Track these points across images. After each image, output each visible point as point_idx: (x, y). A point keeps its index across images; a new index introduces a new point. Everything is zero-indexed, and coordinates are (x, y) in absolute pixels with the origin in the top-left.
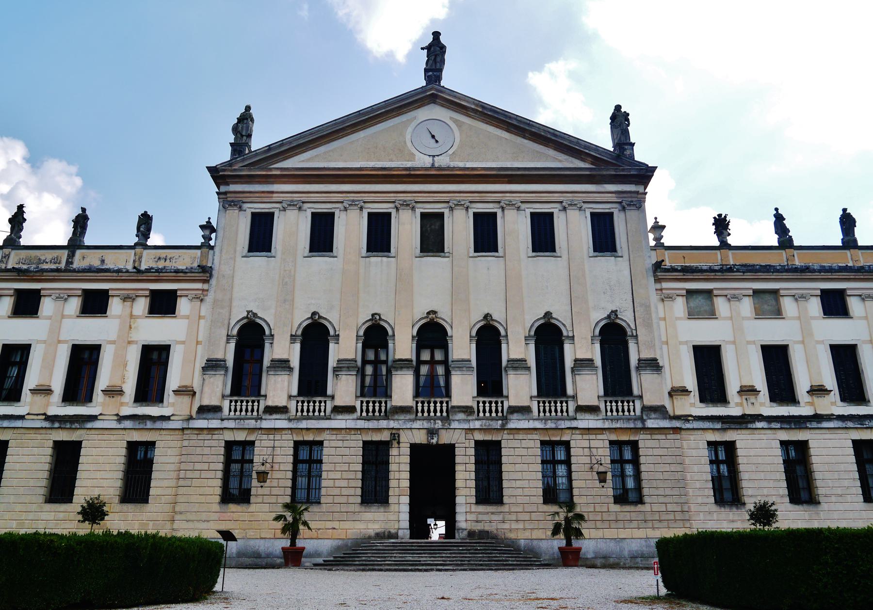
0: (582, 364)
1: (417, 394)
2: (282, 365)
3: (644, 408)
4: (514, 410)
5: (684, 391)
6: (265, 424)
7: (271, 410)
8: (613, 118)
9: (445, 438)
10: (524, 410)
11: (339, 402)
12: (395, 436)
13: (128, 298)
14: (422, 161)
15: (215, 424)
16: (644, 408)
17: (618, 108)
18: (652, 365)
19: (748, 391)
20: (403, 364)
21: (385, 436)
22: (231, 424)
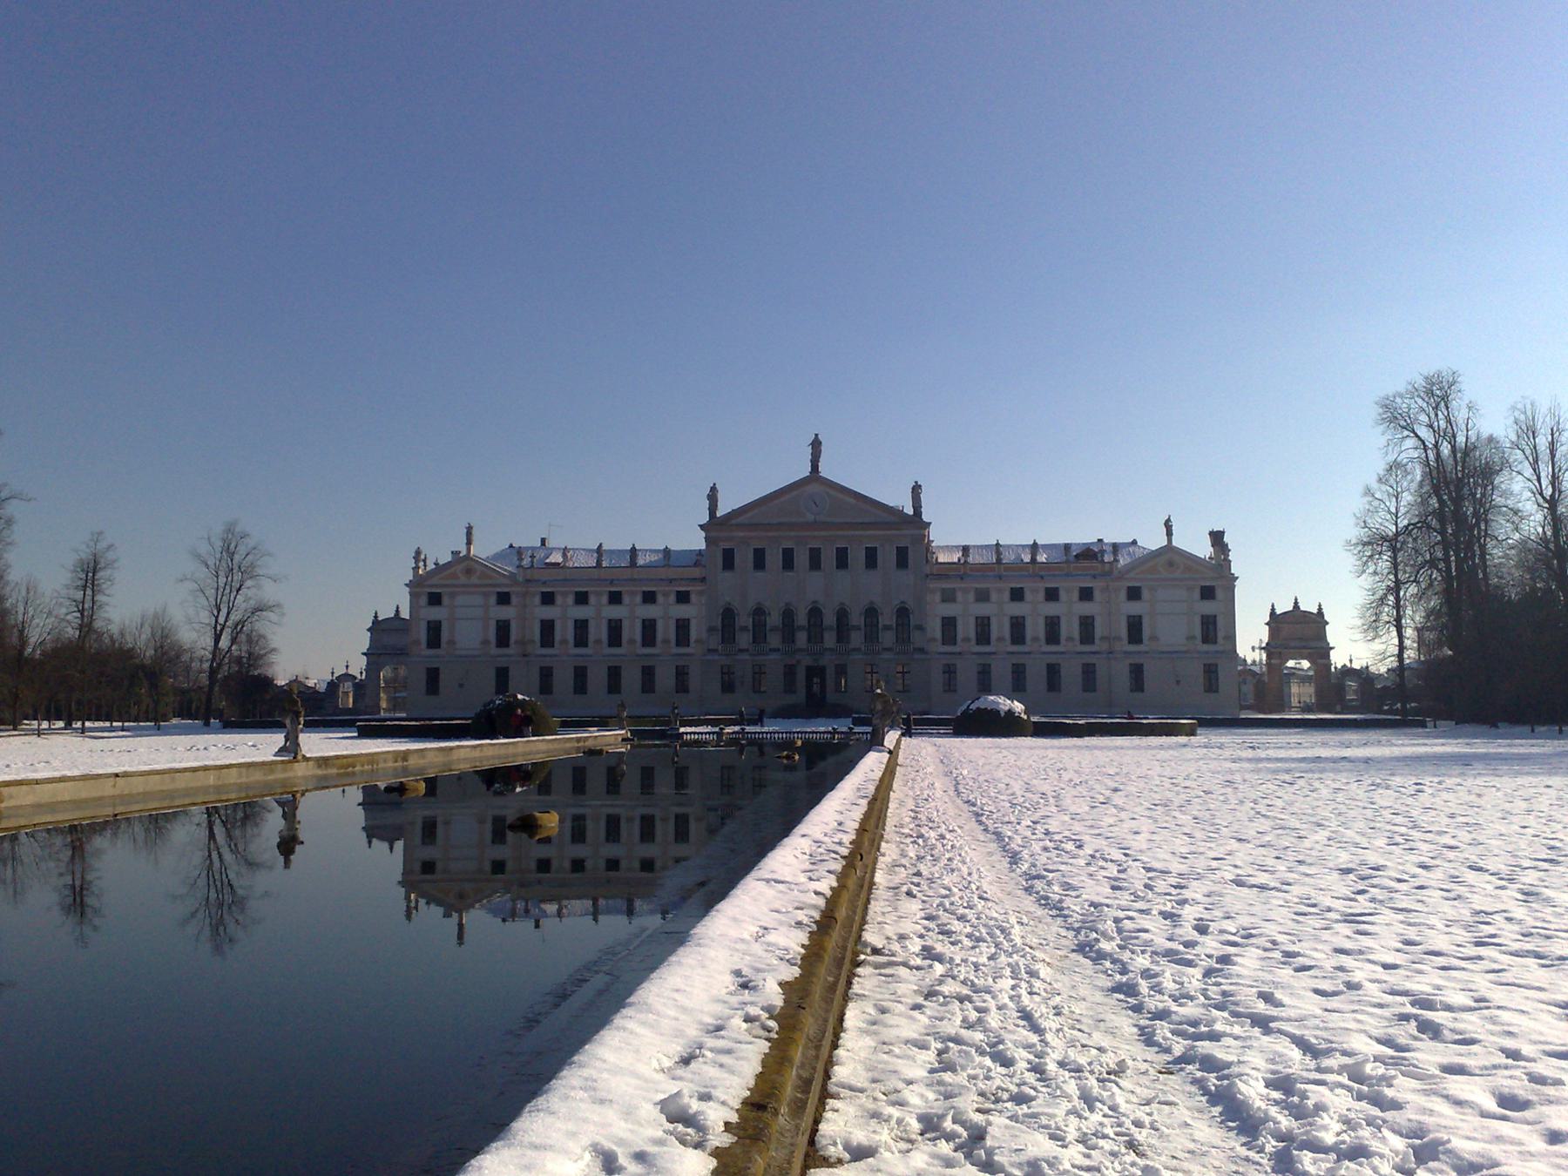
0: (887, 628)
1: (809, 640)
2: (744, 629)
3: (914, 649)
4: (854, 650)
5: (934, 640)
6: (738, 657)
7: (741, 651)
8: (913, 488)
9: (821, 663)
10: (858, 650)
11: (772, 647)
12: (799, 662)
13: (666, 594)
14: (810, 517)
15: (716, 657)
16: (914, 649)
17: (916, 482)
18: (920, 628)
19: (967, 640)
20: (801, 628)
21: (794, 662)
22: (724, 658)
